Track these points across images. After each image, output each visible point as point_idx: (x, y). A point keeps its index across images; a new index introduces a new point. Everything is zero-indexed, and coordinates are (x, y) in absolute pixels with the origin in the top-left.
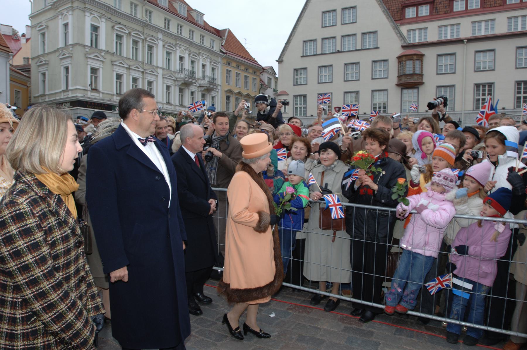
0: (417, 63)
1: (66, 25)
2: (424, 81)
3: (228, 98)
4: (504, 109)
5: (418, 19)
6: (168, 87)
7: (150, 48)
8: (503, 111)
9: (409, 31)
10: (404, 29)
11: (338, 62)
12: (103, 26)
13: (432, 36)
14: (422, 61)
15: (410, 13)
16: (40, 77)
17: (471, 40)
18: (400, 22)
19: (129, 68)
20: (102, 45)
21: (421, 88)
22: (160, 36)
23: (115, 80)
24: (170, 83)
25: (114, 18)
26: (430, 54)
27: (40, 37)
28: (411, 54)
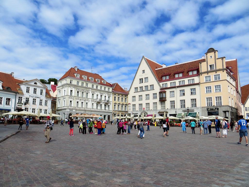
0: (164, 94)
1: (65, 90)
2: (166, 99)
3: (115, 105)
4: (188, 107)
5: (166, 80)
6: (93, 104)
7: (87, 93)
8: (188, 108)
9: (163, 84)
10: (161, 84)
11: (144, 94)
12: (73, 90)
13: (169, 86)
14: (166, 93)
15: (164, 78)
16: (59, 103)
17: (178, 87)
18: (160, 81)
19: (80, 100)
20: (73, 95)
21: (166, 102)
22: (90, 90)
23: (76, 103)
24: (93, 102)
25: (77, 87)
26: (168, 91)
27: (59, 92)
28: (163, 91)
